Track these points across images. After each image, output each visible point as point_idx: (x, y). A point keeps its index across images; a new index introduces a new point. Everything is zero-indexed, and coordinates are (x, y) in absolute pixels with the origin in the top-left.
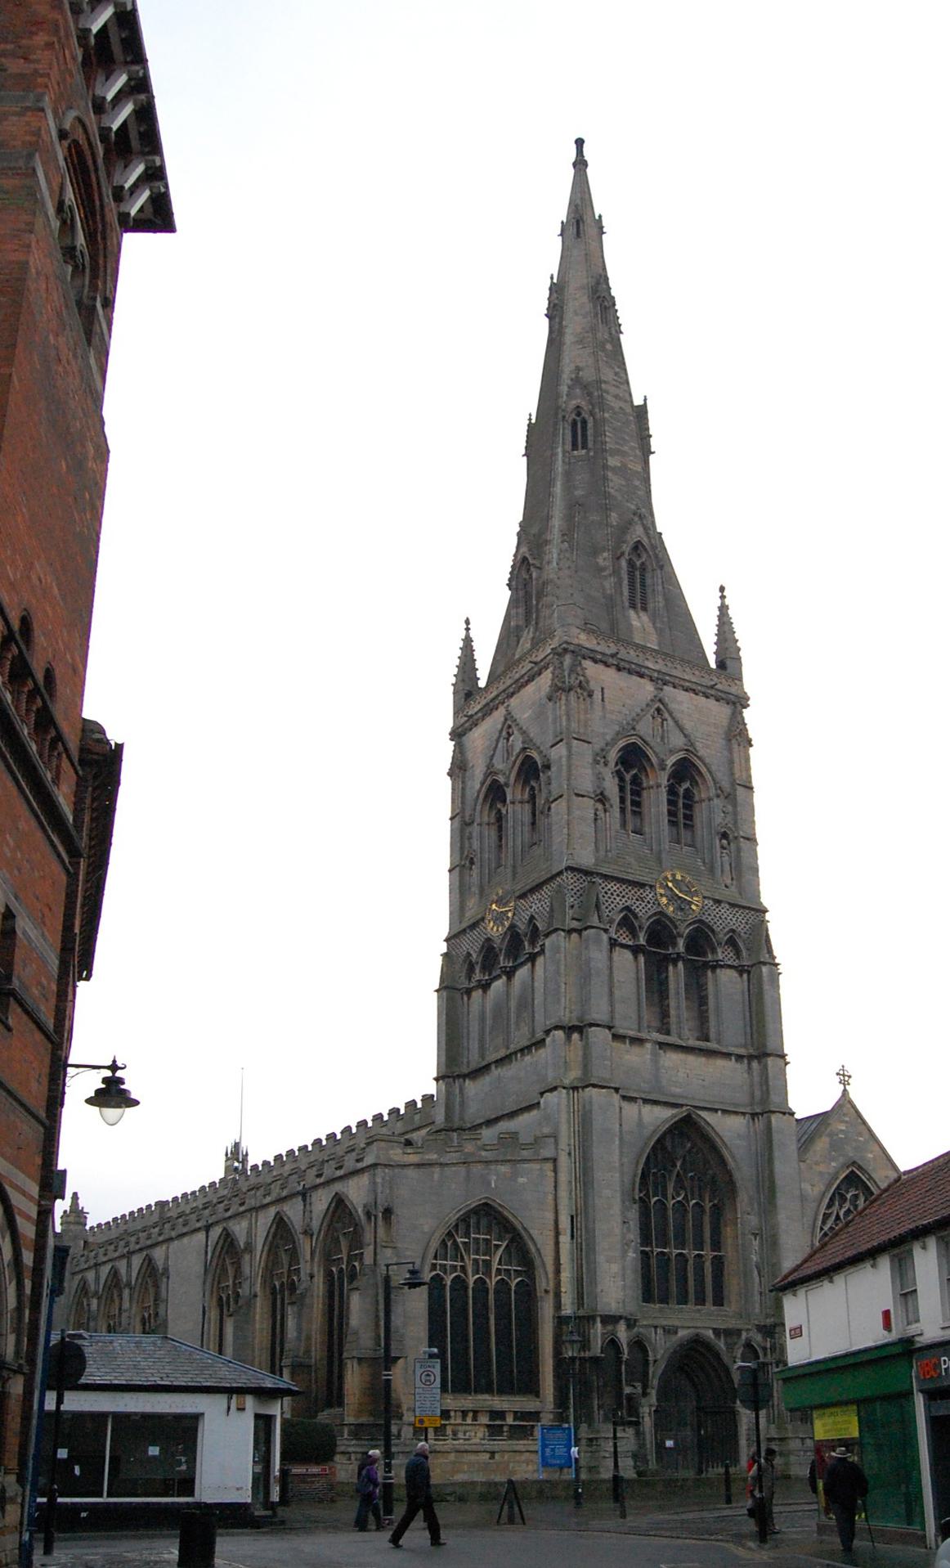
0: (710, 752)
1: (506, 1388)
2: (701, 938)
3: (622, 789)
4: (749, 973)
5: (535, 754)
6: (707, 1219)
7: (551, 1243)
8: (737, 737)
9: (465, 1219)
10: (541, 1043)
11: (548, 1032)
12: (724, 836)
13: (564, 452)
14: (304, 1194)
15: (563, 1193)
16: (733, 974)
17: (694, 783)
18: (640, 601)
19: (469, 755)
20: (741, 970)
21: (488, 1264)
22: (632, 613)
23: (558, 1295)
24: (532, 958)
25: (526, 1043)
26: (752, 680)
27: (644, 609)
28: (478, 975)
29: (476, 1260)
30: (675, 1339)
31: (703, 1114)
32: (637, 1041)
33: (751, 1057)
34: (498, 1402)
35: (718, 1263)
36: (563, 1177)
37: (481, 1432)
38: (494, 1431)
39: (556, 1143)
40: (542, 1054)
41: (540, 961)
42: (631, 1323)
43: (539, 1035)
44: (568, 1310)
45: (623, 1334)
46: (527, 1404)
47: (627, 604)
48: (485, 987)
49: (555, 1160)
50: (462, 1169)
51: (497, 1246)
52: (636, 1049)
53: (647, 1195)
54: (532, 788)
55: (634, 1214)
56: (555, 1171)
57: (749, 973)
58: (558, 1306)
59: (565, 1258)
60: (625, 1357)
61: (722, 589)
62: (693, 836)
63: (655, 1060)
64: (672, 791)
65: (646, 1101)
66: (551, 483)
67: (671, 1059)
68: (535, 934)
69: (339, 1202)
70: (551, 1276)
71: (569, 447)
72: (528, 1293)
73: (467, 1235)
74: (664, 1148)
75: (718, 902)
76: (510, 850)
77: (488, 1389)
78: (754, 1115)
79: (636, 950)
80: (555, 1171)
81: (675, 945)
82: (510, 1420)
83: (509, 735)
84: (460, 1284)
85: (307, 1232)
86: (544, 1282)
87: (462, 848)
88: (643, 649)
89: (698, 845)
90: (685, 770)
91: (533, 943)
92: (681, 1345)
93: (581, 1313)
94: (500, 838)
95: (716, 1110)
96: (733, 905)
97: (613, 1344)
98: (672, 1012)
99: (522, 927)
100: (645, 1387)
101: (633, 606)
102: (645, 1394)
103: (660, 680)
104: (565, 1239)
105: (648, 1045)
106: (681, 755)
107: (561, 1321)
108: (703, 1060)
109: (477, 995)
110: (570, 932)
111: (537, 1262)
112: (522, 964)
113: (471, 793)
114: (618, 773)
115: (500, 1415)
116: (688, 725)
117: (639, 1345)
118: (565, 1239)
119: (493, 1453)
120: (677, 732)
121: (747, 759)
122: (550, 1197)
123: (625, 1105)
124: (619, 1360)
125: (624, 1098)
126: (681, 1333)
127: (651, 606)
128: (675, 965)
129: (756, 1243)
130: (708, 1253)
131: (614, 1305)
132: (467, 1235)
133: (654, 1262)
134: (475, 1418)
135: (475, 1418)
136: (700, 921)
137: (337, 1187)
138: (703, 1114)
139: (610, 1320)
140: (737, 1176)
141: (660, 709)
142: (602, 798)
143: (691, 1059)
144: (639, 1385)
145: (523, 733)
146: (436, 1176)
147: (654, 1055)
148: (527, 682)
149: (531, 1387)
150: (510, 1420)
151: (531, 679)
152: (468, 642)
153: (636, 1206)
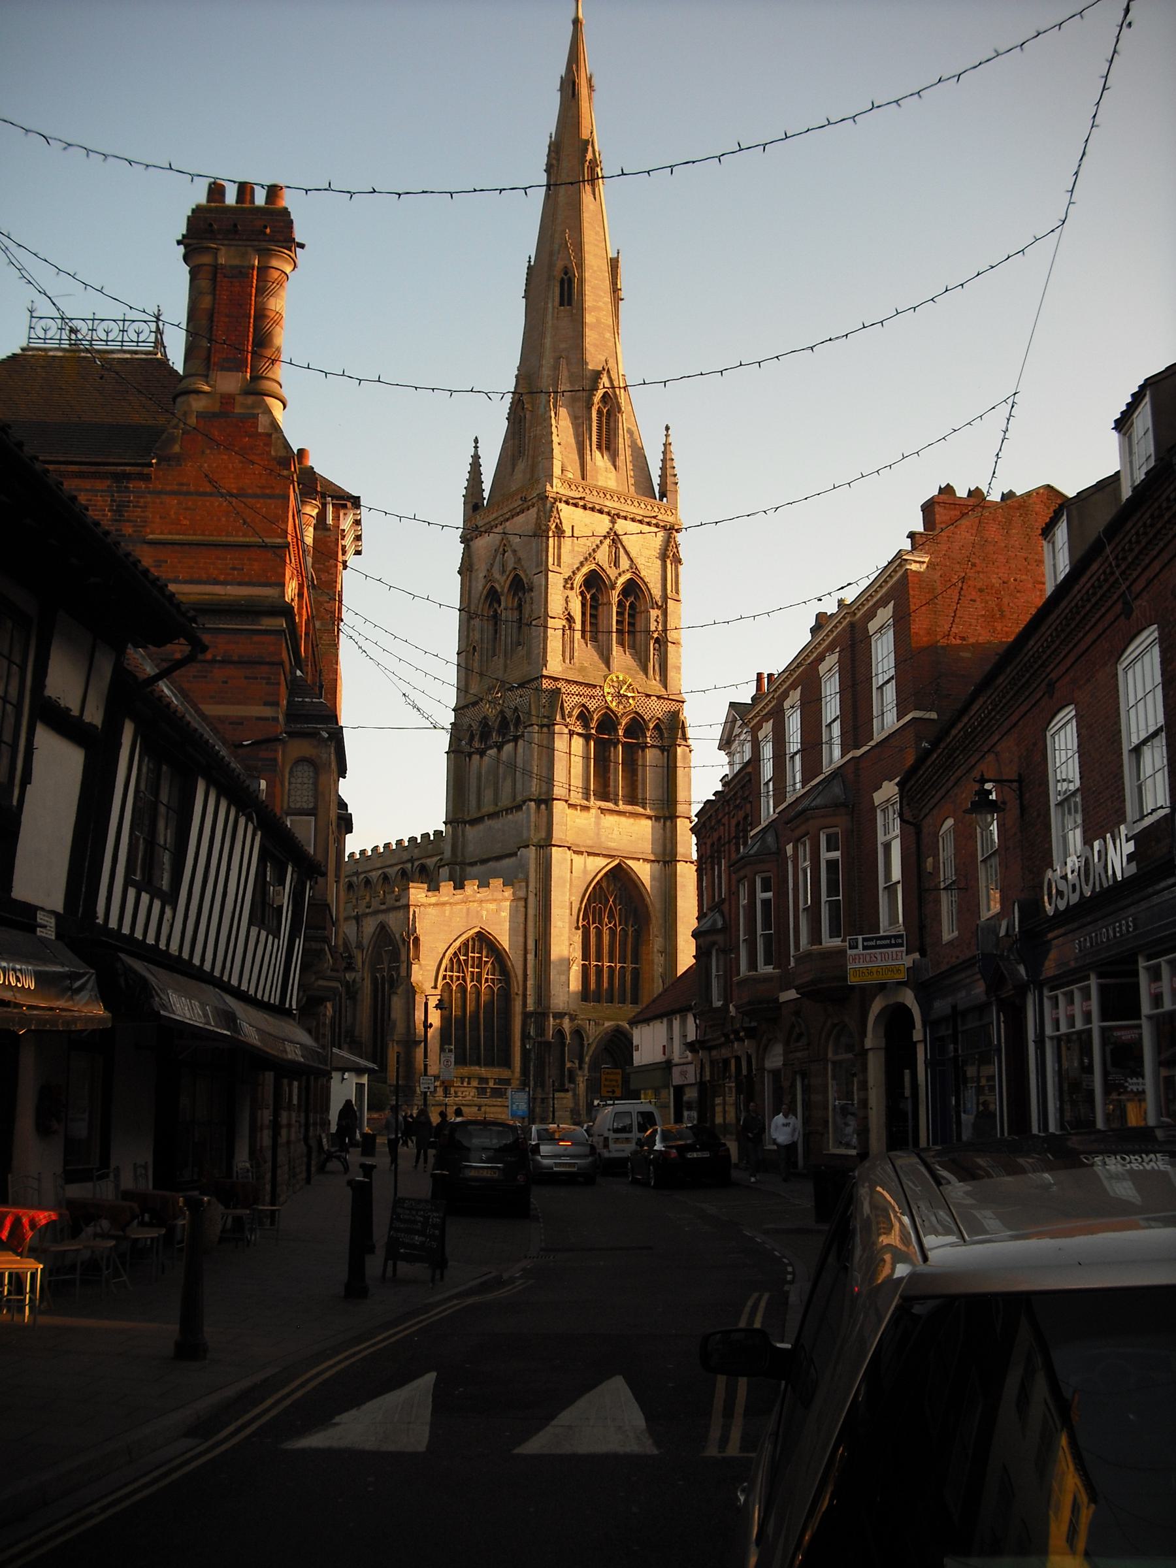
0: (651, 573)
1: (490, 1063)
2: (637, 726)
3: (583, 614)
4: (668, 751)
5: (523, 576)
6: (630, 940)
7: (521, 959)
8: (669, 555)
9: (465, 944)
10: (519, 808)
11: (524, 802)
12: (657, 641)
13: (553, 308)
14: (358, 919)
15: (531, 924)
16: (657, 752)
17: (637, 597)
18: (608, 445)
19: (475, 560)
20: (662, 749)
21: (480, 974)
22: (597, 454)
23: (525, 996)
24: (516, 739)
25: (510, 805)
26: (689, 505)
27: (608, 448)
28: (476, 744)
29: (472, 973)
30: (601, 1028)
31: (629, 862)
32: (586, 808)
33: (666, 819)
34: (483, 1071)
35: (636, 974)
36: (531, 912)
37: (473, 1092)
38: (481, 1091)
39: (527, 887)
40: (519, 816)
41: (520, 742)
42: (573, 1018)
43: (519, 798)
44: (530, 1008)
45: (566, 1024)
46: (505, 1073)
47: (594, 447)
48: (482, 753)
49: (526, 900)
50: (463, 907)
51: (487, 962)
52: (585, 814)
53: (588, 923)
54: (520, 599)
55: (578, 937)
56: (526, 907)
57: (668, 751)
58: (525, 1004)
59: (530, 972)
60: (568, 1041)
61: (667, 428)
62: (634, 641)
63: (598, 824)
64: (620, 603)
65: (589, 854)
66: (542, 335)
67: (610, 820)
68: (518, 721)
69: (382, 927)
70: (521, 983)
71: (557, 299)
72: (506, 995)
73: (466, 954)
74: (601, 887)
75: (649, 696)
76: (503, 643)
77: (478, 1064)
78: (665, 862)
79: (587, 737)
80: (526, 907)
81: (616, 730)
82: (491, 1084)
83: (505, 552)
84: (463, 989)
85: (360, 946)
86: (516, 988)
87: (468, 636)
88: (604, 492)
89: (638, 646)
90: (634, 588)
91: (516, 726)
92: (606, 1034)
93: (539, 1010)
94: (496, 632)
95: (639, 859)
96: (659, 697)
97: (560, 1033)
98: (612, 784)
99: (509, 714)
100: (581, 1062)
101: (599, 447)
102: (581, 1068)
103: (614, 517)
104: (531, 957)
105: (593, 811)
106: (628, 576)
107: (526, 1016)
108: (631, 820)
109: (476, 757)
110: (542, 726)
111: (513, 974)
112: (509, 741)
113: (474, 601)
114: (582, 593)
115: (484, 1080)
116: (633, 555)
117: (578, 1033)
118: (531, 957)
119: (480, 1107)
120: (625, 557)
121: (677, 576)
122: (522, 926)
123: (575, 856)
124: (563, 1044)
125: (575, 852)
126: (607, 1024)
127: (612, 446)
128: (616, 747)
129: (662, 959)
130: (629, 966)
131: (561, 1005)
132: (466, 954)
133: (593, 970)
134: (469, 1083)
135: (469, 1083)
136: (636, 713)
137: (381, 917)
138: (629, 862)
139: (559, 1016)
140: (651, 908)
141: (615, 539)
142: (570, 619)
143: (623, 820)
144: (577, 1062)
145: (514, 551)
146: (447, 913)
147: (597, 817)
148: (518, 514)
149: (507, 1063)
150: (491, 1084)
151: (522, 511)
152: (476, 457)
153: (580, 932)
